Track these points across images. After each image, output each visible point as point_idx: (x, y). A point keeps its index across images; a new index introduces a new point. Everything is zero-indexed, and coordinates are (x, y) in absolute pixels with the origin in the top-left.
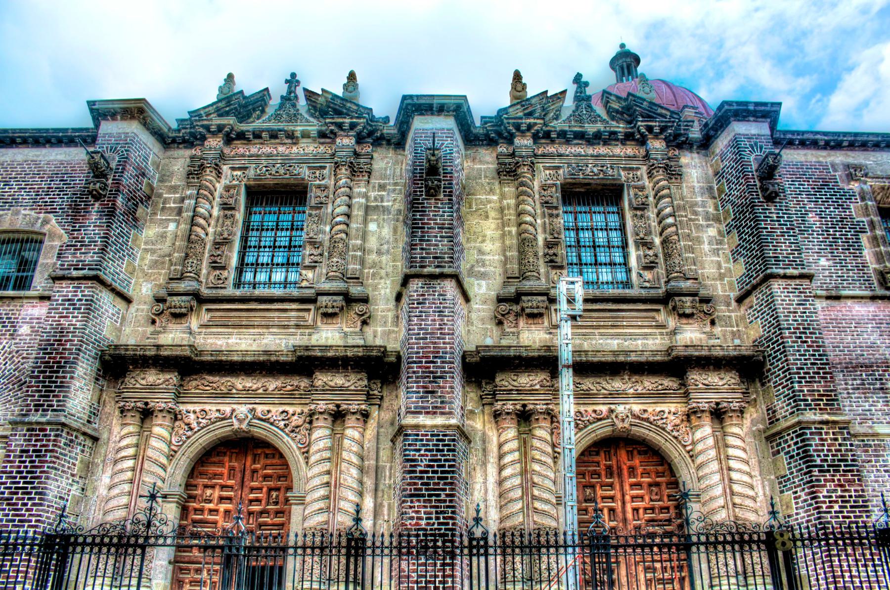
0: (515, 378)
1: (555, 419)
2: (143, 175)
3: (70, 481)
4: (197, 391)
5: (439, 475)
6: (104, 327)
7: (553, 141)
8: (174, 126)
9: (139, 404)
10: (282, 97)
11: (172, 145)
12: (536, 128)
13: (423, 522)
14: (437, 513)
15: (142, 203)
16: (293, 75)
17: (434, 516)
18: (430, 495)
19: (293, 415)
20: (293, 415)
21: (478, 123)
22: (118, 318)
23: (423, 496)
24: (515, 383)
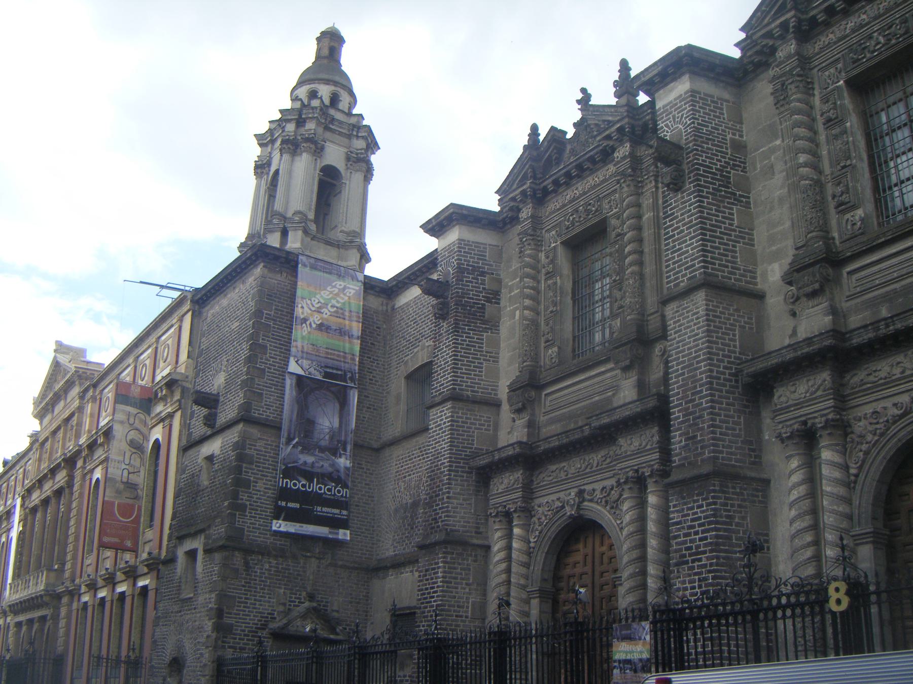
0: (793, 389)
1: (849, 430)
2: (483, 274)
3: (467, 590)
4: (544, 483)
5: (700, 536)
6: (473, 440)
7: (827, 24)
8: (497, 209)
9: (500, 509)
10: (575, 125)
11: (506, 228)
12: (791, 25)
13: (688, 593)
14: (700, 580)
15: (491, 302)
16: (584, 91)
17: (696, 584)
18: (693, 561)
19: (612, 489)
20: (612, 489)
21: (736, 54)
22: (489, 426)
23: (687, 562)
24: (793, 396)
